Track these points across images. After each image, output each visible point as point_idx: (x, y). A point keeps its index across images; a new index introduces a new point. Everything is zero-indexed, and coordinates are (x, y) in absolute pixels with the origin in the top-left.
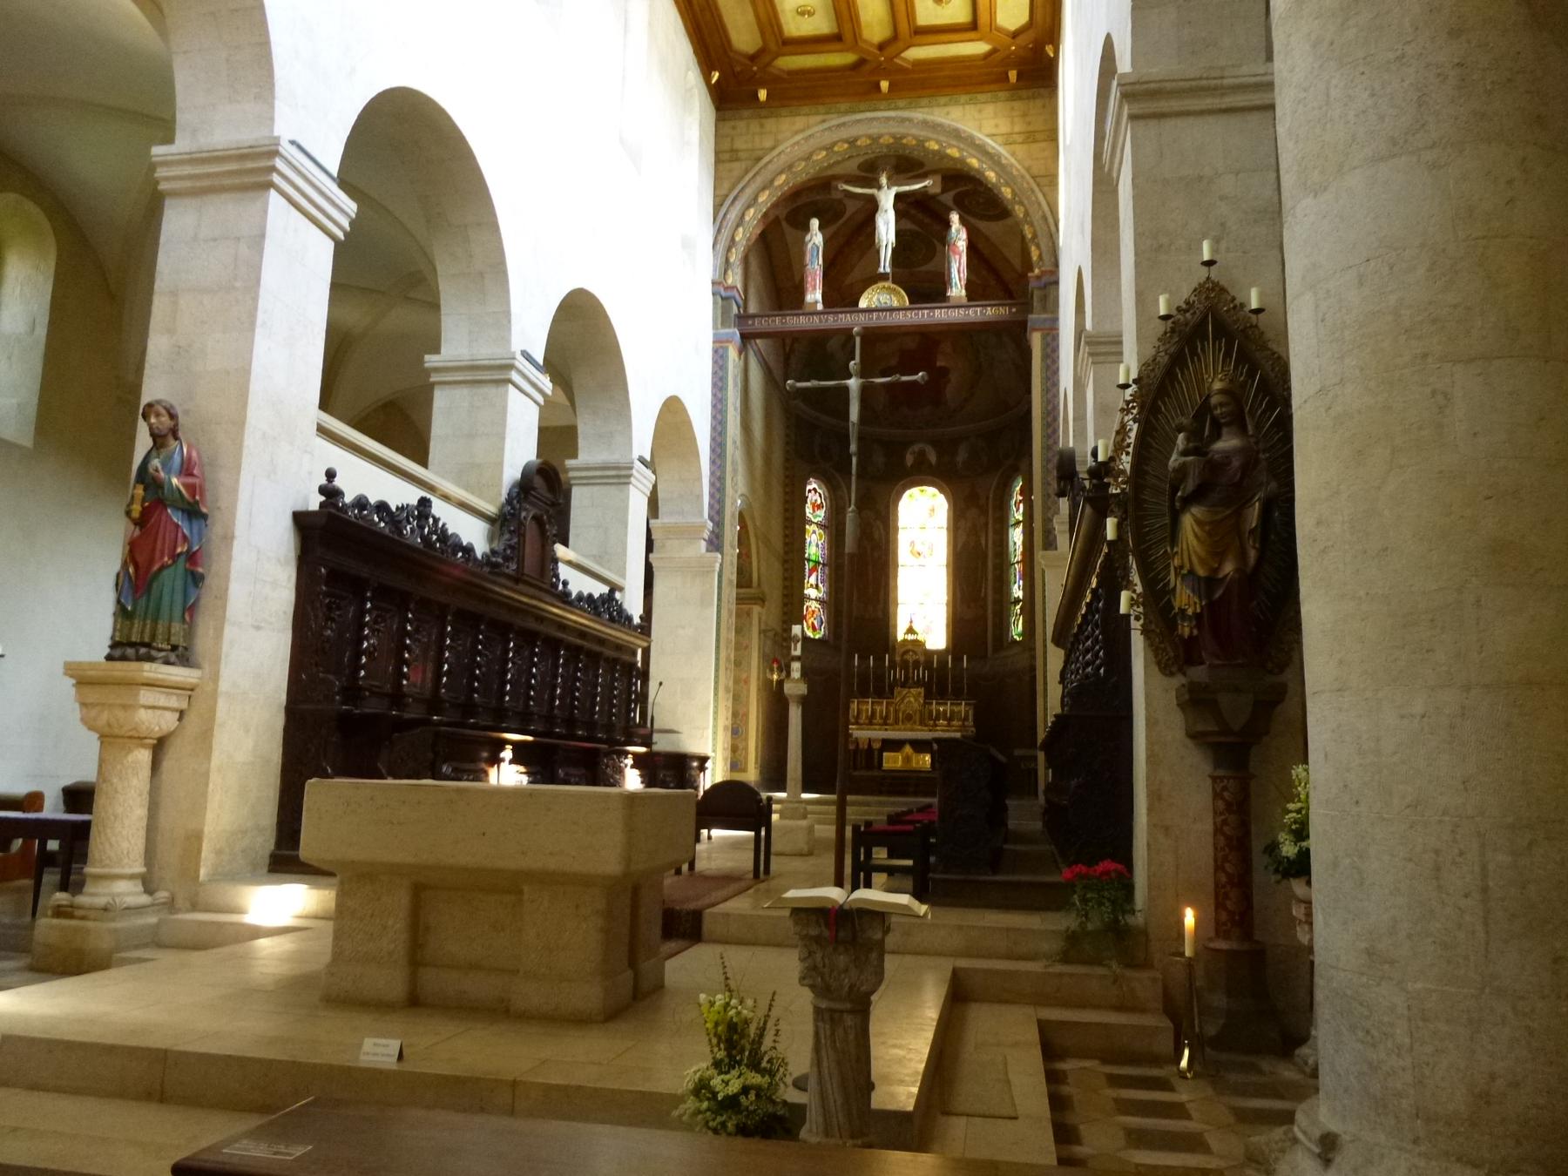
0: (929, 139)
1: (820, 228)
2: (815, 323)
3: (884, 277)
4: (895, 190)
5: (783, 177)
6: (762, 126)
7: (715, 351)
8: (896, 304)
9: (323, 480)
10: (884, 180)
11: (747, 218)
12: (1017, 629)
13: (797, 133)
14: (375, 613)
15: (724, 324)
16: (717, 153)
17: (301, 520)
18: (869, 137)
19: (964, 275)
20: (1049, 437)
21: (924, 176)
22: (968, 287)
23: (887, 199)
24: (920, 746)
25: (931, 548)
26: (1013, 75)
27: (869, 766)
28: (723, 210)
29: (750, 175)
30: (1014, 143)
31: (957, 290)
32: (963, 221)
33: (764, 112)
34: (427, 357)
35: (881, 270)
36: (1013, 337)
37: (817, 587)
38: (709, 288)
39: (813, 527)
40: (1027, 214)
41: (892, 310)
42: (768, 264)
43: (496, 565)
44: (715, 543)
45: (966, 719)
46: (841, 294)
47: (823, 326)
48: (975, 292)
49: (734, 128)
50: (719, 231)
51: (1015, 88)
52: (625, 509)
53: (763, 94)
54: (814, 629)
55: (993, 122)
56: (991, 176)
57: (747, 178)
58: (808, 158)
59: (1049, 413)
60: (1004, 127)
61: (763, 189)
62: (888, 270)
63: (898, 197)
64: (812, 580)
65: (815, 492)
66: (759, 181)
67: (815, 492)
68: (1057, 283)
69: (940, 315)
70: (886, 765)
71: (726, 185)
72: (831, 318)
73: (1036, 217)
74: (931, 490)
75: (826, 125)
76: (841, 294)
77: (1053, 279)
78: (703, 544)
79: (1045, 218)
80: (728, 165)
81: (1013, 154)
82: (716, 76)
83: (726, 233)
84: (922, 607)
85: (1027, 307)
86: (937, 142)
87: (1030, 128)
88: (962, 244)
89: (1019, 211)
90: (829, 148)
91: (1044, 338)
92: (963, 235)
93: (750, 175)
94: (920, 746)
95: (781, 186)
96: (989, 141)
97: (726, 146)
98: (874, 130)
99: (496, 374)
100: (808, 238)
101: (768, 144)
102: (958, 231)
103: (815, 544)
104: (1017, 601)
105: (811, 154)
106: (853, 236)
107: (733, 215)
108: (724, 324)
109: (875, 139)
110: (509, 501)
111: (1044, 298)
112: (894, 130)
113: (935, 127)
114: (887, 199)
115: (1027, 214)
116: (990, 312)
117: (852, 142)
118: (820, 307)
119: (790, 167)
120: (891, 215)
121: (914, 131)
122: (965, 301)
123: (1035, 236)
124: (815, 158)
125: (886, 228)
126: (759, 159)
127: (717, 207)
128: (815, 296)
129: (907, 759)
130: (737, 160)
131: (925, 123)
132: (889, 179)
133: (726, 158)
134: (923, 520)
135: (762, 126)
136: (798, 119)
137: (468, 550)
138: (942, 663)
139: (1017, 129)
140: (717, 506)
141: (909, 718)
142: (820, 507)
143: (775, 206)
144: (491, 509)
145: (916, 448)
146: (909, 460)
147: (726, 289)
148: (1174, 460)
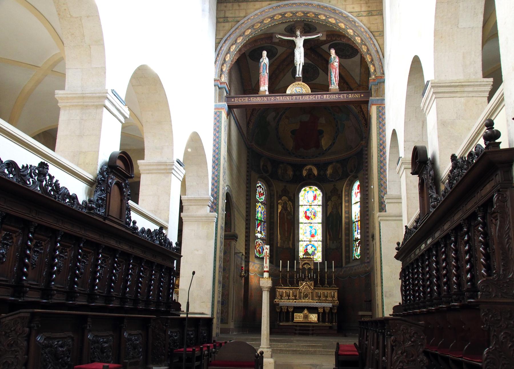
0: (320, 14)
1: (267, 56)
2: (265, 101)
3: (299, 79)
4: (304, 38)
5: (250, 31)
6: (239, 6)
7: (216, 113)
8: (304, 91)
10: (298, 33)
11: (232, 50)
12: (357, 253)
13: (256, 10)
14: (35, 241)
15: (219, 101)
16: (217, 18)
18: (291, 12)
19: (337, 79)
20: (381, 156)
23: (300, 42)
24: (312, 310)
25: (315, 215)
27: (287, 320)
28: (220, 45)
29: (234, 29)
30: (362, 16)
31: (334, 86)
32: (336, 53)
34: (57, 92)
35: (297, 76)
36: (362, 107)
37: (261, 233)
38: (213, 83)
39: (260, 204)
40: (368, 50)
41: (302, 95)
42: (241, 74)
43: (92, 208)
44: (214, 208)
45: (334, 297)
46: (277, 86)
47: (268, 102)
49: (226, 7)
50: (218, 55)
52: (169, 187)
54: (260, 253)
55: (352, 6)
56: (351, 32)
57: (232, 30)
58: (261, 22)
59: (381, 145)
60: (357, 9)
61: (240, 36)
62: (301, 76)
63: (305, 41)
64: (259, 229)
65: (261, 188)
66: (238, 32)
67: (261, 188)
68: (384, 82)
69: (326, 98)
70: (295, 320)
71: (222, 34)
72: (272, 98)
73: (373, 52)
74: (314, 188)
75: (270, 6)
76: (277, 86)
77: (382, 80)
78: (209, 208)
79: (377, 51)
80: (223, 24)
81: (361, 21)
83: (221, 57)
85: (369, 94)
86: (325, 16)
87: (370, 9)
88: (336, 64)
89: (364, 49)
90: (272, 18)
91: (377, 109)
92: (337, 60)
93: (234, 29)
94: (312, 310)
95: (248, 35)
96: (349, 15)
97: (222, 15)
98: (294, 10)
99: (96, 102)
100: (261, 60)
101: (242, 14)
102: (334, 58)
103: (260, 212)
104: (357, 239)
105: (263, 20)
107: (225, 48)
108: (219, 101)
109: (294, 14)
110: (101, 173)
111: (377, 90)
112: (303, 10)
113: (324, 8)
114: (300, 42)
115: (368, 50)
116: (350, 96)
117: (283, 15)
118: (267, 93)
119: (253, 26)
120: (302, 50)
121: (313, 10)
122: (338, 91)
123: (372, 60)
124: (265, 22)
125: (300, 57)
127: (217, 44)
128: (264, 88)
129: (306, 317)
130: (227, 22)
131: (319, 5)
132: (301, 33)
133: (221, 20)
134: (310, 200)
135: (239, 6)
136: (257, 3)
137: (74, 198)
138: (322, 269)
139: (364, 9)
140: (215, 190)
141: (306, 296)
142: (262, 194)
143: (245, 46)
144: (90, 177)
145: (308, 167)
146: (305, 173)
147: (221, 83)
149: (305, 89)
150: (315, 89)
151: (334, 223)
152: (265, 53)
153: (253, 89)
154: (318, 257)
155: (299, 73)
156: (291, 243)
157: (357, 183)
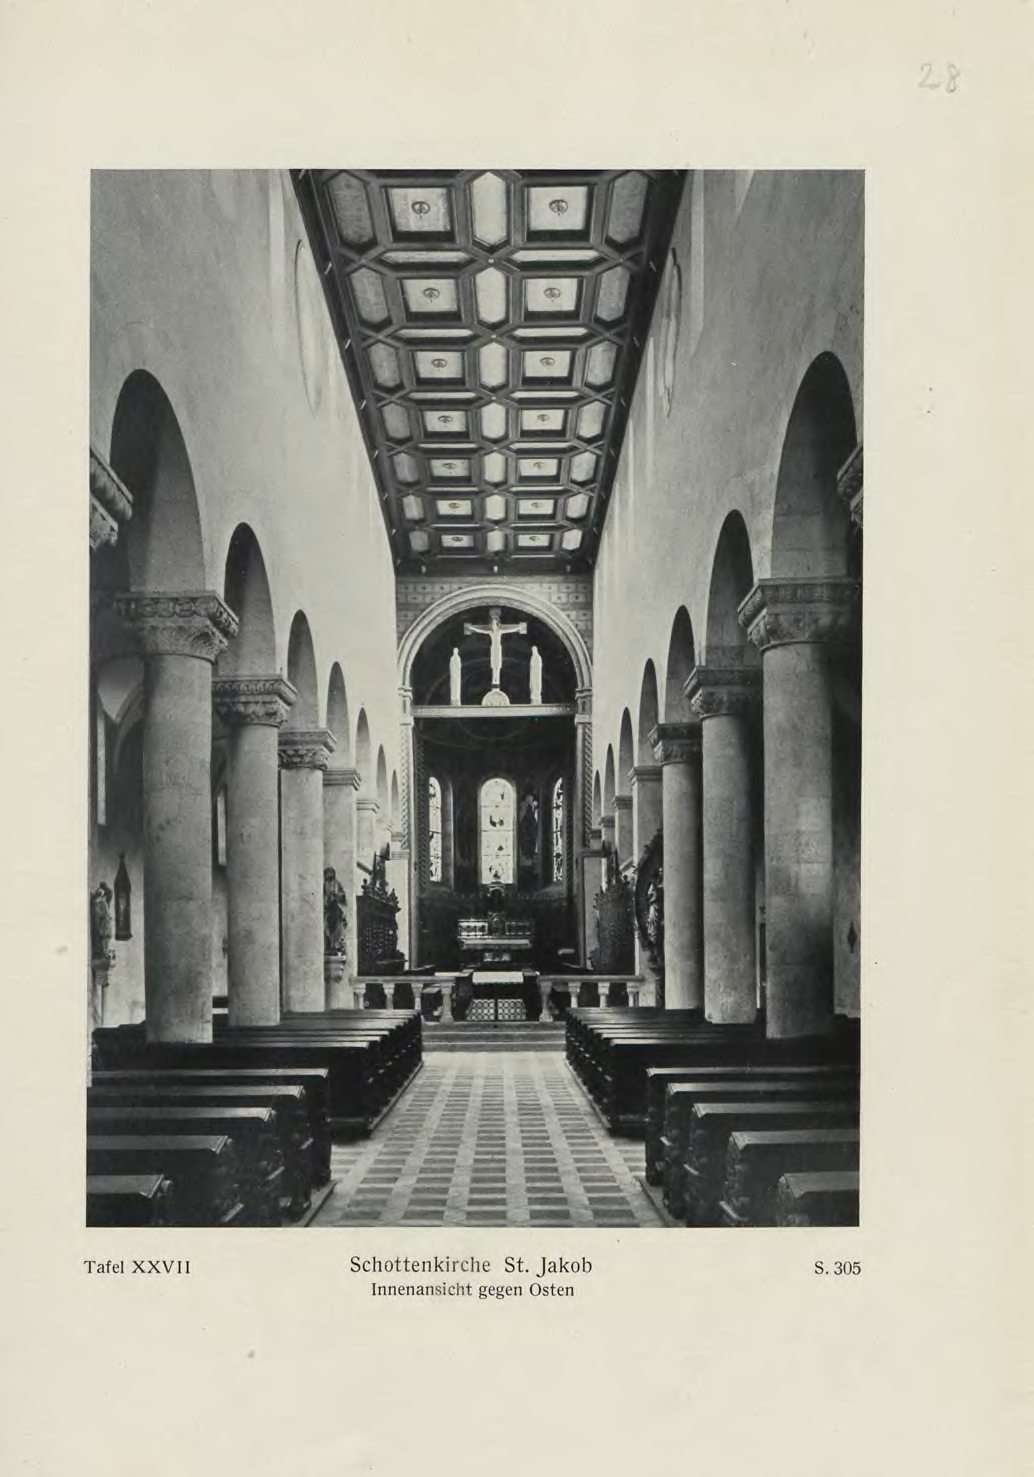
1: (459, 654)
3: (496, 686)
9: (362, 883)
17: (358, 898)
21: (516, 621)
22: (543, 694)
26: (569, 568)
28: (403, 641)
33: (426, 579)
35: (494, 682)
46: (472, 697)
48: (547, 698)
51: (571, 573)
53: (424, 569)
74: (502, 782)
76: (472, 697)
82: (399, 562)
84: (498, 861)
101: (428, 599)
106: (476, 655)
118: (459, 703)
126: (423, 610)
134: (498, 798)
147: (405, 691)
148: (650, 891)
149: (505, 699)
150: (514, 700)
151: (530, 833)
152: (456, 651)
153: (443, 698)
154: (508, 878)
155: (496, 680)
156: (473, 861)
157: (560, 781)
